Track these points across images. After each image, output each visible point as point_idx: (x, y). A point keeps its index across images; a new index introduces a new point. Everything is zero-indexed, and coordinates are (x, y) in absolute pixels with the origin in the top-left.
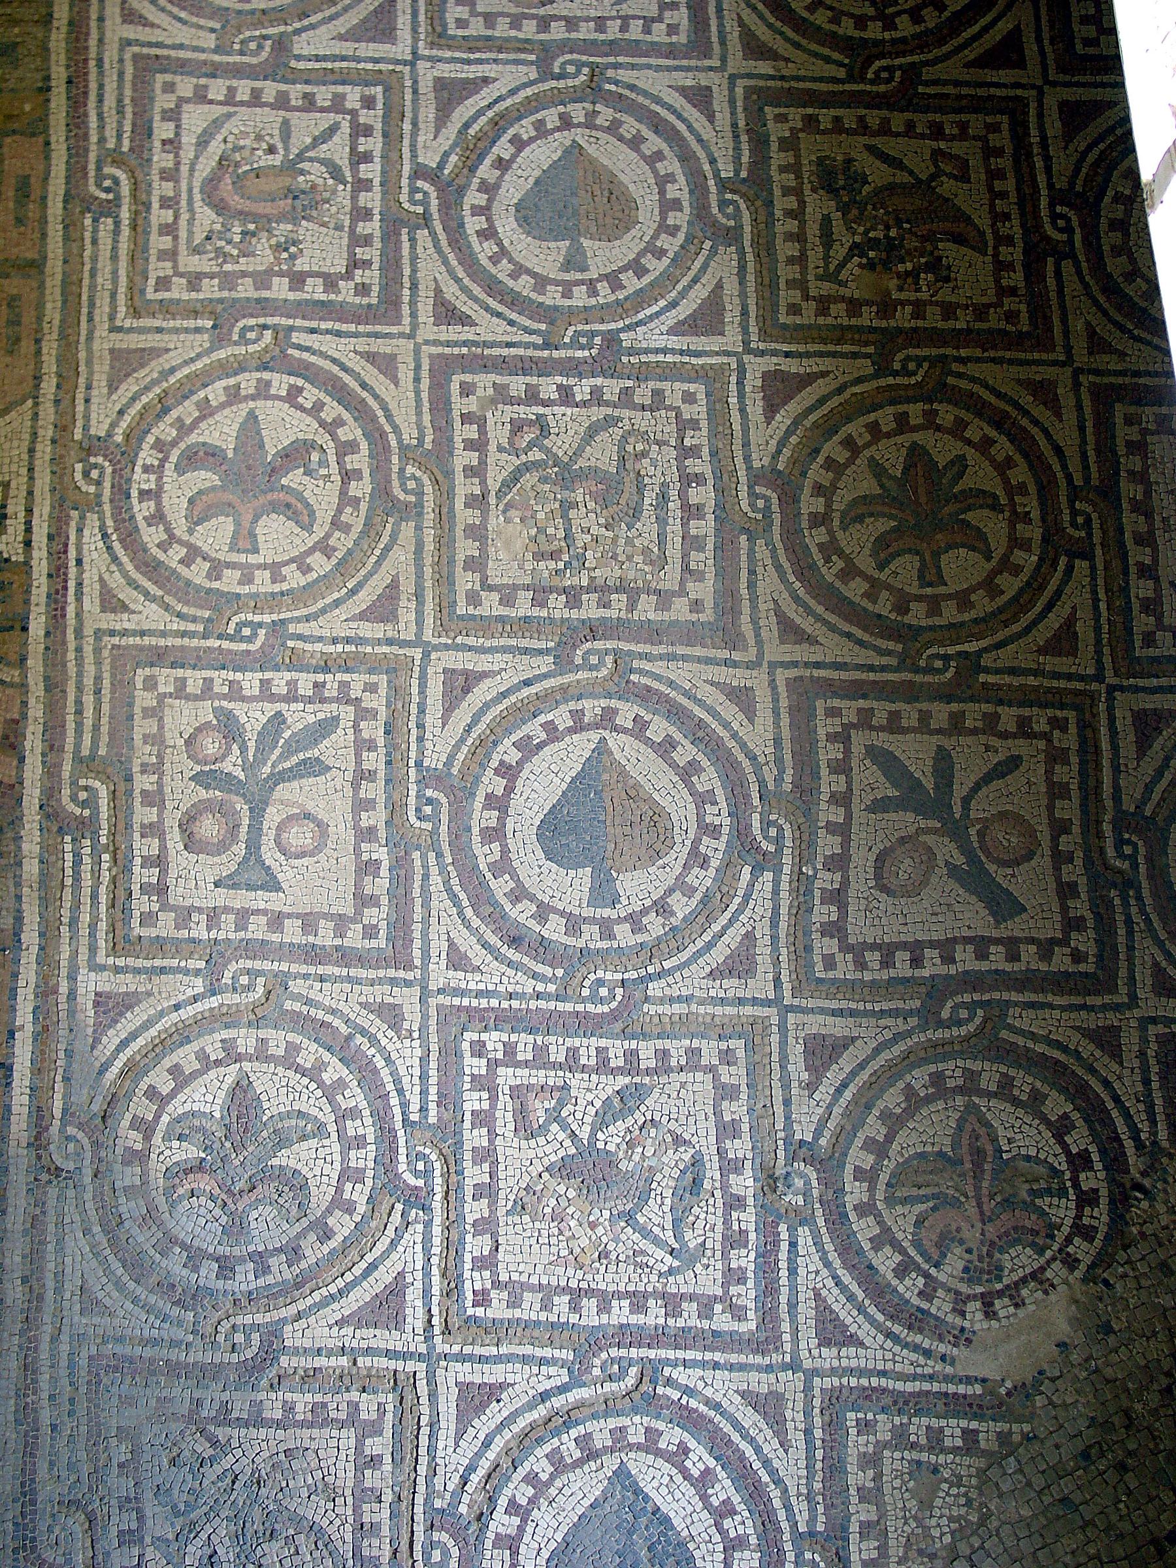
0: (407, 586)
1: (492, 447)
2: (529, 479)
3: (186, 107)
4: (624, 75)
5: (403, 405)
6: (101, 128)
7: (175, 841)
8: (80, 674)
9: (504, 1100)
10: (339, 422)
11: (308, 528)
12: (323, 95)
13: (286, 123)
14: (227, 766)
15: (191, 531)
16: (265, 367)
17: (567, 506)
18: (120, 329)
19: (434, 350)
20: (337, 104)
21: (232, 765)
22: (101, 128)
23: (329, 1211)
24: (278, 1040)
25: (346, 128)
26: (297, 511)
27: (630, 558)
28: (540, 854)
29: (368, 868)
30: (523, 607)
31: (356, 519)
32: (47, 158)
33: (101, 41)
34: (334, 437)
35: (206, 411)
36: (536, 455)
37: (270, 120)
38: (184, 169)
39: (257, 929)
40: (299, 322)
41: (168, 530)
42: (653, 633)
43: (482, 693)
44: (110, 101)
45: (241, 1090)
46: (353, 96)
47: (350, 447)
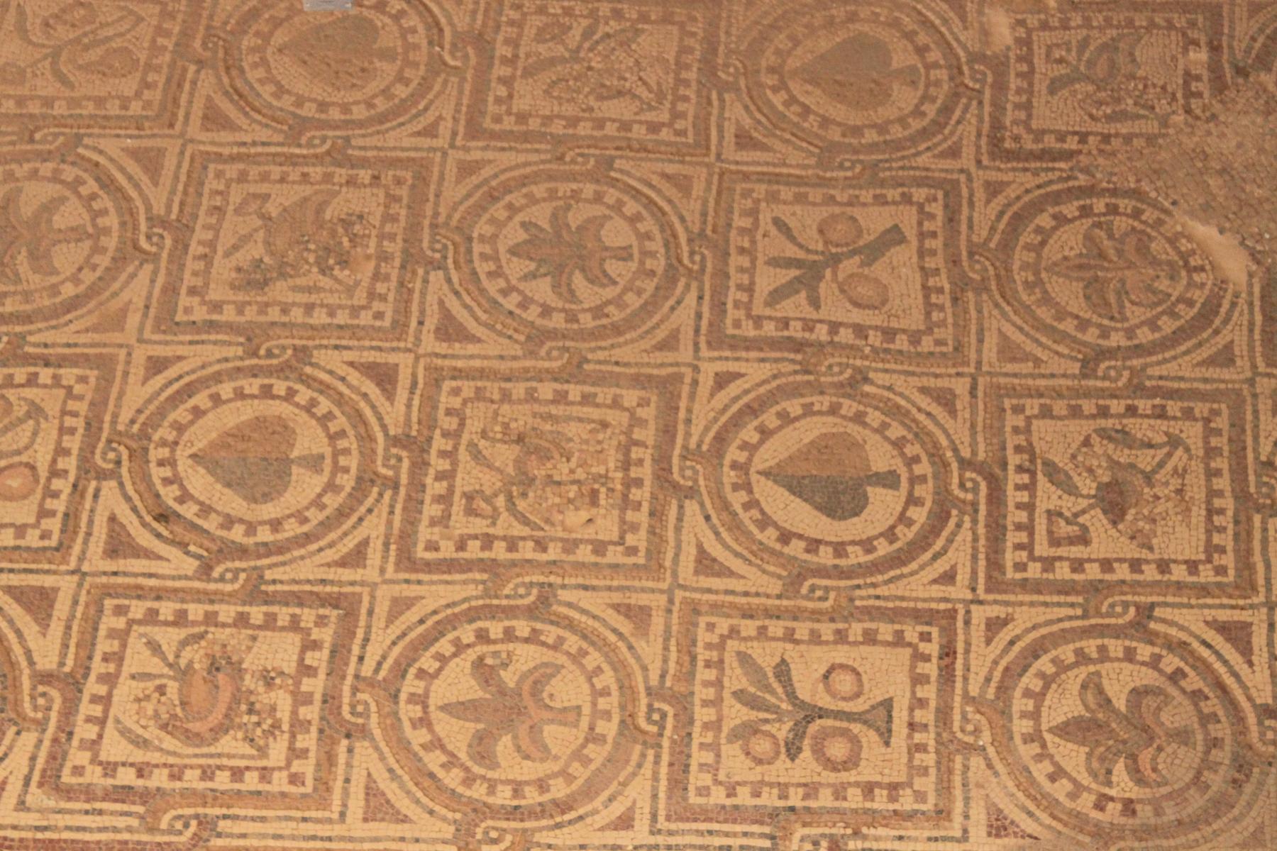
0: (617, 598)
1: (491, 531)
2: (521, 505)
4: (125, 416)
5: (438, 594)
7: (851, 776)
9: (1061, 551)
10: (457, 643)
11: (559, 668)
15: (556, 758)
16: (395, 697)
17: (550, 481)
18: (343, 815)
19: (390, 568)
20: (122, 636)
21: (782, 731)
22: (115, 830)
23: (1161, 671)
24: (1020, 704)
25: (142, 629)
27: (599, 442)
28: (855, 520)
29: (870, 638)
30: (642, 517)
31: (551, 633)
35: (437, 744)
36: (501, 501)
38: (171, 760)
39: (926, 716)
40: (351, 670)
41: (555, 775)
42: (668, 432)
43: (716, 550)
44: (86, 821)
45: (1063, 730)
46: (110, 621)
47: (482, 636)
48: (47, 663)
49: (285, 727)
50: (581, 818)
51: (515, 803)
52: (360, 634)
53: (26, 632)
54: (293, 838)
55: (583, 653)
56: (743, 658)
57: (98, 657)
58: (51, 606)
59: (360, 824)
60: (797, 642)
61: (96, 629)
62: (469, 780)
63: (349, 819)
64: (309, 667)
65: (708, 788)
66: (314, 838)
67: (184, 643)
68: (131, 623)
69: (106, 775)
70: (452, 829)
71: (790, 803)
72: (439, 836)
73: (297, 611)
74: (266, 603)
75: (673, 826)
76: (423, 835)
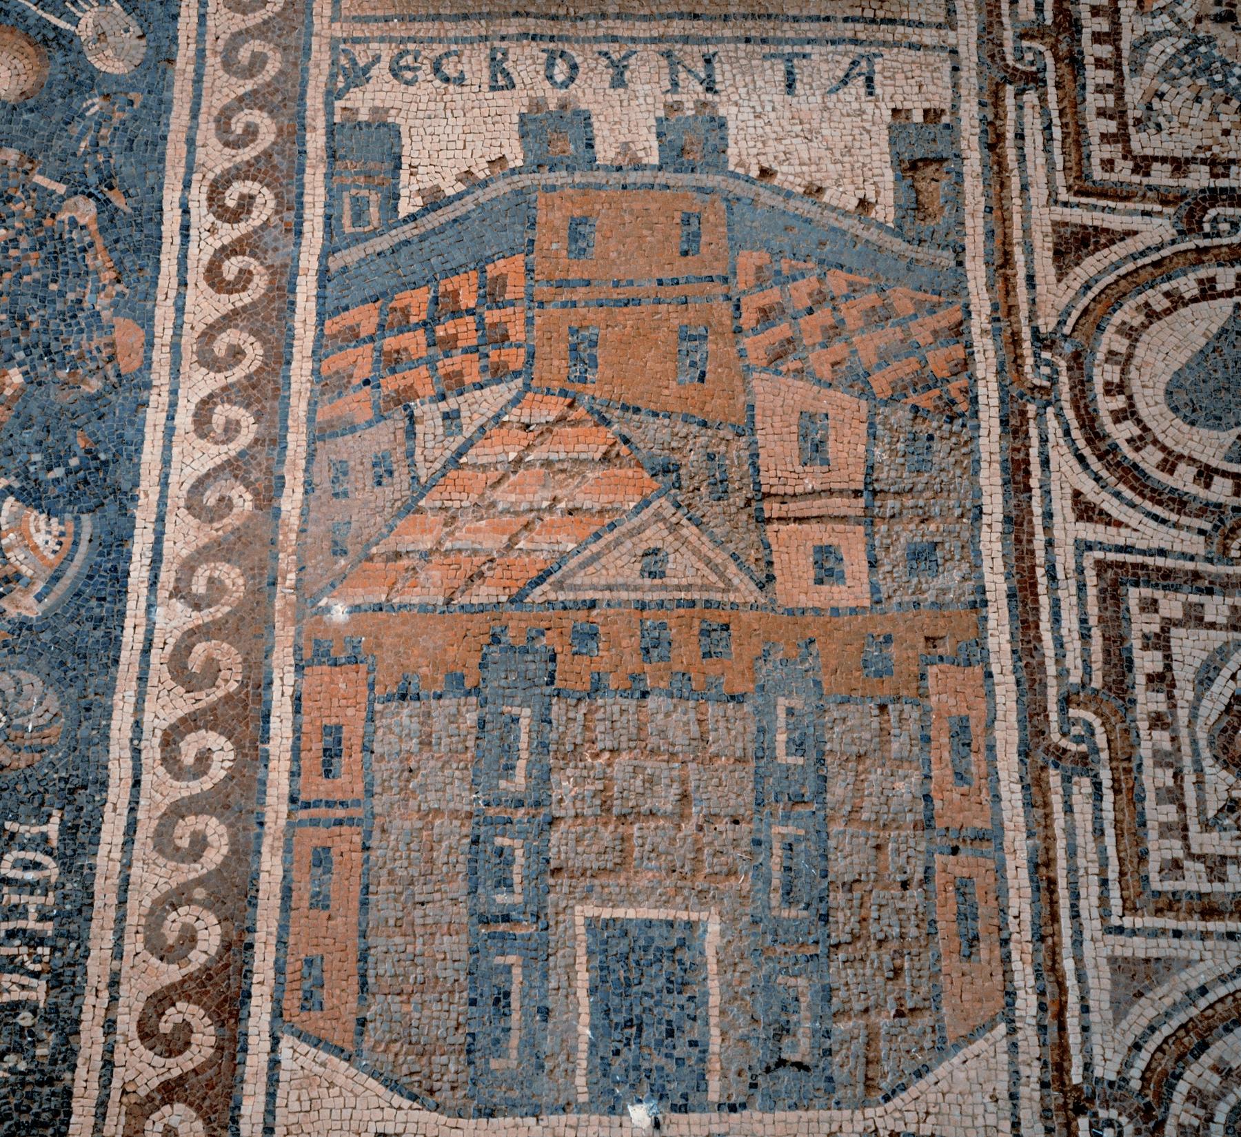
3: (1174, 632)
6: (1060, 659)
18: (1120, 930)
22: (1060, 659)
32: (991, 694)
33: (1050, 544)
38: (1183, 714)
44: (1070, 621)
54: (1072, 870)
59: (1107, 952)
63: (1110, 938)
66: (1075, 896)
70: (1113, 1077)
72: (1098, 1059)
76: (1096, 1039)
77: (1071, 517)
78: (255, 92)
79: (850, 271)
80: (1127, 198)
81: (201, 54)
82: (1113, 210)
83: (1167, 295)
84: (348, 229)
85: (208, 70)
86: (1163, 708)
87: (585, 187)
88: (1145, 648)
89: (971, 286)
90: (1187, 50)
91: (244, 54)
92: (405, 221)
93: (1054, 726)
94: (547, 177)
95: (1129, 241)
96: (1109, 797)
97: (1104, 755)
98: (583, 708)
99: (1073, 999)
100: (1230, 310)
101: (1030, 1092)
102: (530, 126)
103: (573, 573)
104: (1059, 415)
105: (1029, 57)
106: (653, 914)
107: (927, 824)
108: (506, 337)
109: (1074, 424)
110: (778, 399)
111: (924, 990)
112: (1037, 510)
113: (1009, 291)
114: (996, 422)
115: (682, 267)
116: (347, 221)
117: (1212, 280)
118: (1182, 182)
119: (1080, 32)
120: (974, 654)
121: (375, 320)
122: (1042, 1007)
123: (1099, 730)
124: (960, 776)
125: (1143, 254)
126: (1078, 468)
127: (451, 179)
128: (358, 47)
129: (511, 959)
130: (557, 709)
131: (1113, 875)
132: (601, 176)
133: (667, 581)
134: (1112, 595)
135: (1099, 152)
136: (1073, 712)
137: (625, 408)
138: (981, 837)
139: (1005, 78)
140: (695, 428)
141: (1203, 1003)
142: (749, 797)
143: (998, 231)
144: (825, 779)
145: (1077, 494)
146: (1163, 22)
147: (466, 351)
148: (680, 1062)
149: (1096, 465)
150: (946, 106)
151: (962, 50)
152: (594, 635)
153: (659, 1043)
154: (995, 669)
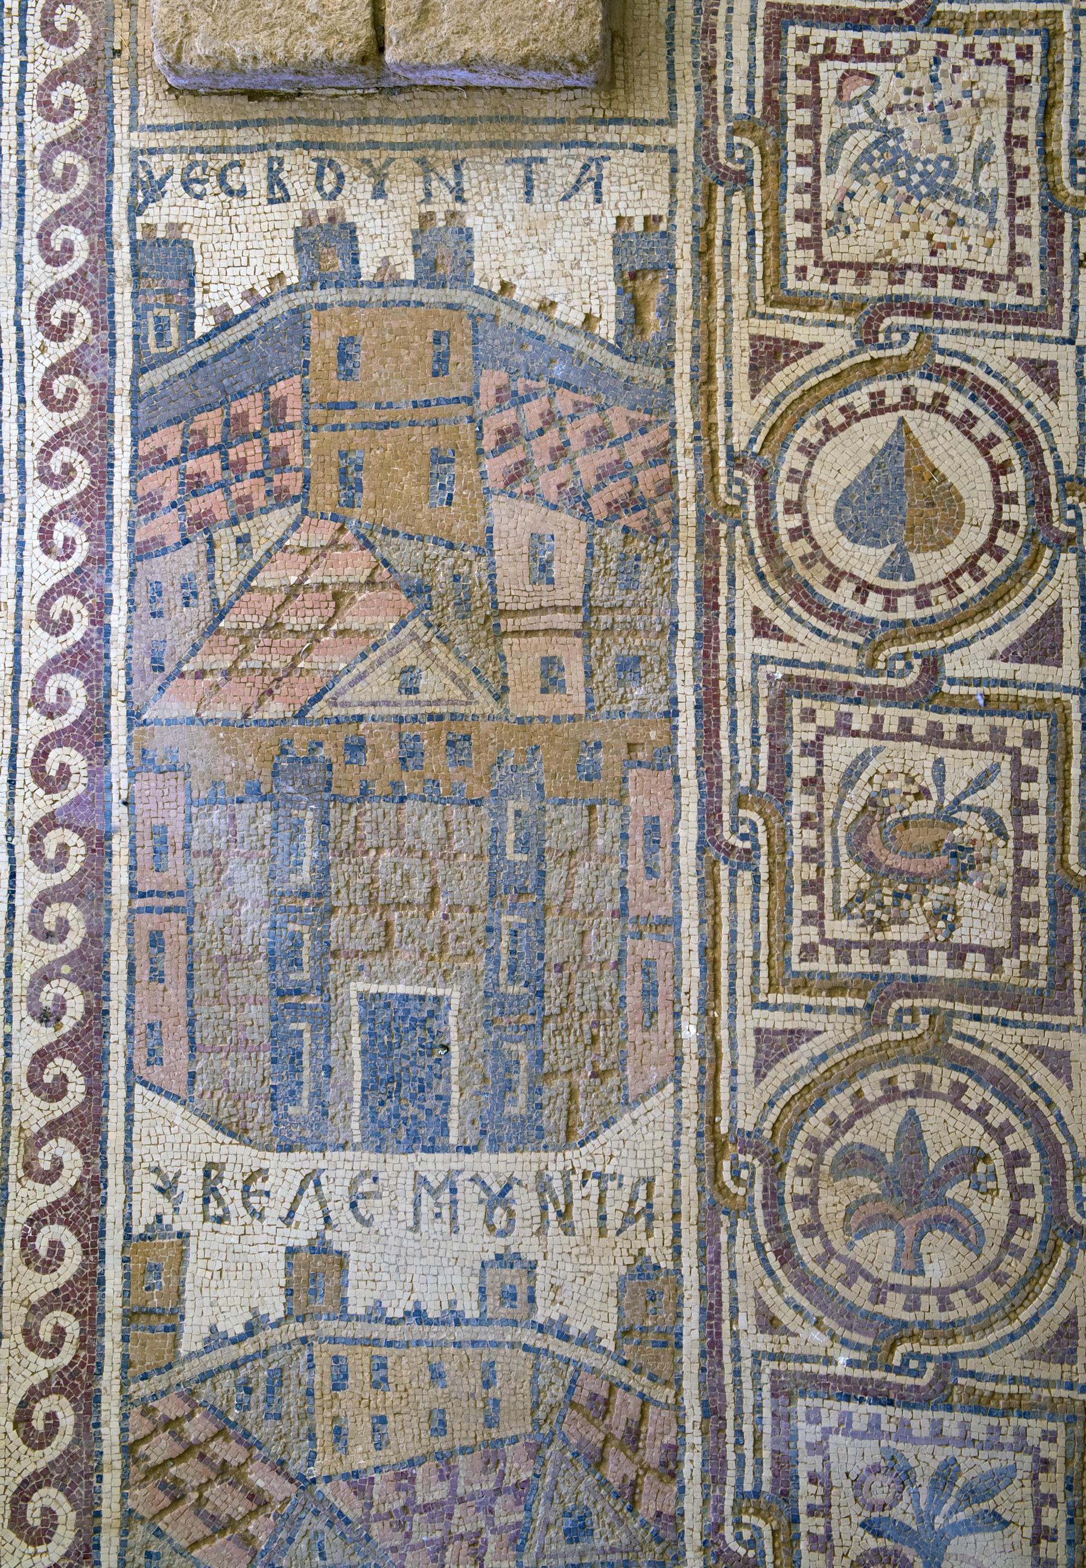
3: (827, 740)
6: (734, 763)
8: (739, 1401)
10: (1007, 1128)
12: (980, 726)
13: (939, 761)
14: (896, 1513)
15: (851, 1245)
18: (765, 1006)
20: (996, 742)
21: (903, 1513)
22: (734, 763)
25: (1006, 766)
26: (962, 1228)
31: (1029, 1241)
32: (678, 796)
33: (731, 658)
34: (1002, 1144)
35: (862, 1108)
37: (921, 759)
38: (828, 814)
40: (959, 1007)
41: (826, 1243)
44: (744, 730)
46: (1014, 730)
47: (1017, 1159)
48: (952, 665)
49: (878, 936)
50: (771, 1273)
51: (788, 1198)
52: (1011, 1015)
53: (997, 635)
54: (732, 954)
55: (1000, 1279)
56: (1006, 1475)
57: (963, 720)
58: (1034, 661)
59: (752, 1025)
60: (1035, 1541)
61: (1003, 714)
62: (814, 1145)
63: (757, 1013)
64: (963, 958)
65: (818, 1421)
66: (733, 976)
67: (989, 815)
68: (1015, 753)
69: (804, 745)
70: (749, 1128)
71: (803, 1517)
72: (740, 1114)
73: (1043, 941)
74: (1052, 904)
75: (765, 1378)
76: (740, 1097)
77: (750, 633)
78: (69, 207)
79: (576, 390)
80: (813, 308)
81: (21, 164)
82: (802, 321)
83: (843, 410)
84: (154, 350)
85: (28, 183)
86: (812, 809)
87: (351, 305)
88: (802, 754)
89: (677, 403)
90: (877, 142)
91: (57, 168)
92: (200, 342)
93: (726, 825)
94: (319, 295)
95: (815, 354)
96: (765, 889)
97: (764, 850)
98: (354, 812)
99: (725, 1063)
100: (894, 425)
101: (688, 1139)
102: (306, 240)
103: (344, 691)
104: (745, 534)
105: (739, 154)
106: (409, 990)
107: (622, 912)
108: (286, 461)
109: (758, 543)
110: (513, 521)
111: (612, 1055)
112: (723, 627)
113: (710, 408)
114: (693, 543)
115: (436, 388)
116: (151, 340)
117: (882, 393)
118: (864, 289)
119: (785, 125)
120: (664, 759)
121: (179, 442)
122: (702, 1071)
123: (761, 829)
124: (650, 871)
125: (825, 368)
126: (758, 586)
127: (238, 297)
128: (155, 159)
129: (302, 1026)
130: (334, 815)
131: (763, 957)
132: (364, 293)
133: (420, 697)
134: (779, 708)
135: (796, 257)
136: (742, 813)
137: (385, 532)
138: (664, 922)
139: (719, 178)
140: (442, 550)
141: (822, 1068)
142: (483, 890)
143: (704, 346)
144: (543, 874)
145: (756, 611)
146: (859, 114)
147: (255, 475)
148: (429, 1112)
149: (773, 584)
150: (664, 212)
151: (680, 148)
152: (362, 747)
153: (413, 1097)
154: (682, 773)
